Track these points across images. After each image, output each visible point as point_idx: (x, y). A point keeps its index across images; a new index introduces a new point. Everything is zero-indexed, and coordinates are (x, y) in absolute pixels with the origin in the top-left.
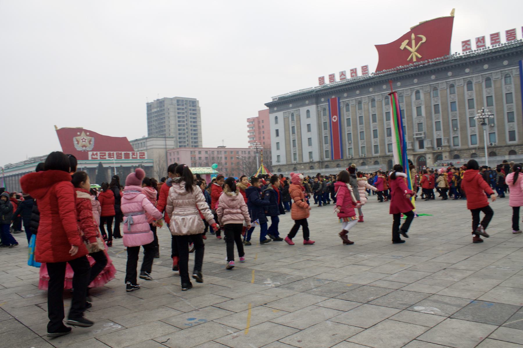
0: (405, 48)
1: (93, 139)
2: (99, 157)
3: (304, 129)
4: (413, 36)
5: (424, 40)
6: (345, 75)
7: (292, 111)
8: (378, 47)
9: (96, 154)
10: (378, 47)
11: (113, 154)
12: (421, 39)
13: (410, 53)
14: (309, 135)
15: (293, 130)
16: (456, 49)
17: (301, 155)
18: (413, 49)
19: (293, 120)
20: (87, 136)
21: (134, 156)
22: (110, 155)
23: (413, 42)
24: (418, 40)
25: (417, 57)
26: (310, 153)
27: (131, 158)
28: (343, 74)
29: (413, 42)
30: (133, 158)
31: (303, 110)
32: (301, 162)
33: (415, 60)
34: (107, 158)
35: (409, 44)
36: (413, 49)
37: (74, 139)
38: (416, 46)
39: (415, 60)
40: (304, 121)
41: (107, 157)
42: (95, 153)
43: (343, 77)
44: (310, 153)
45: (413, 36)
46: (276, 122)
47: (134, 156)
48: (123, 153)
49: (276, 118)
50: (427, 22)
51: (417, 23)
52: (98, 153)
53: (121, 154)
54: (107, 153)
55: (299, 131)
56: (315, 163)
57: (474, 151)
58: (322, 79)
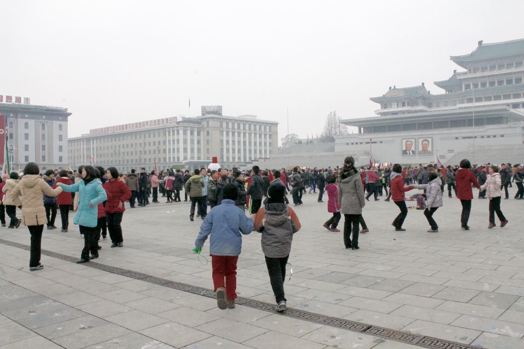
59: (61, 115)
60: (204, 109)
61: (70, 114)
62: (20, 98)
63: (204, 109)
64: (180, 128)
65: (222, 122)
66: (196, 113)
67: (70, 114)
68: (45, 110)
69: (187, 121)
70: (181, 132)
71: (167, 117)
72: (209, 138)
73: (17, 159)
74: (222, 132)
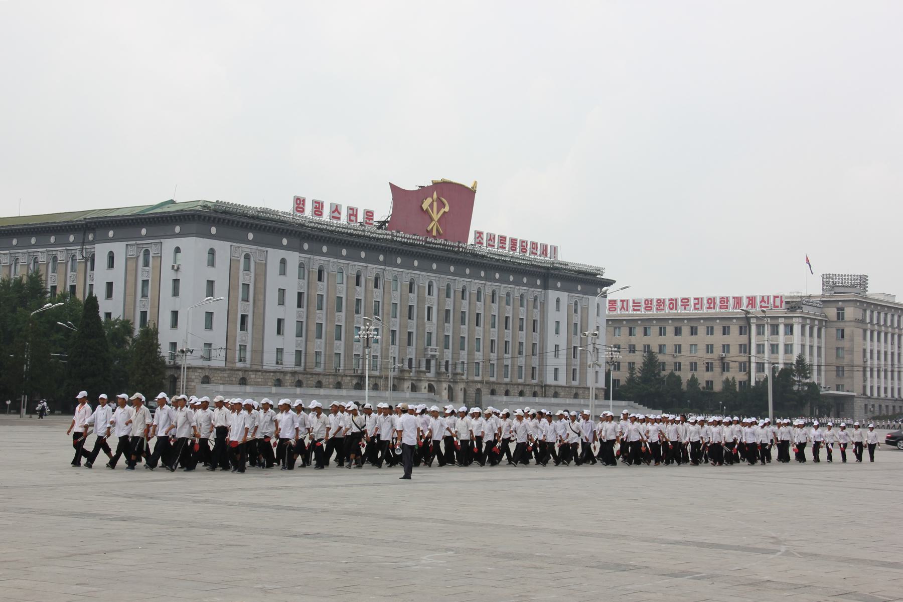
0: (427, 210)
3: (272, 296)
4: (435, 196)
5: (447, 209)
6: (340, 213)
7: (246, 248)
8: (394, 188)
10: (394, 188)
12: (444, 206)
13: (432, 219)
14: (280, 312)
15: (249, 293)
16: (471, 240)
17: (259, 351)
18: (436, 216)
19: (247, 269)
23: (435, 204)
24: (441, 205)
25: (437, 230)
26: (280, 351)
28: (336, 210)
29: (435, 204)
31: (274, 255)
32: (259, 368)
33: (434, 233)
35: (431, 205)
36: (436, 216)
38: (438, 213)
39: (434, 233)
40: (274, 281)
43: (336, 214)
44: (280, 351)
45: (435, 196)
46: (283, 272)
49: (212, 252)
50: (451, 183)
51: (438, 179)
55: (261, 297)
56: (285, 373)
57: (479, 386)
58: (299, 203)
59: (590, 282)
60: (826, 278)
61: (610, 283)
62: (546, 246)
63: (826, 278)
64: (794, 320)
65: (865, 311)
66: (815, 289)
67: (610, 283)
68: (580, 272)
69: (794, 305)
70: (797, 329)
71: (765, 293)
72: (846, 344)
73: (541, 375)
74: (865, 331)
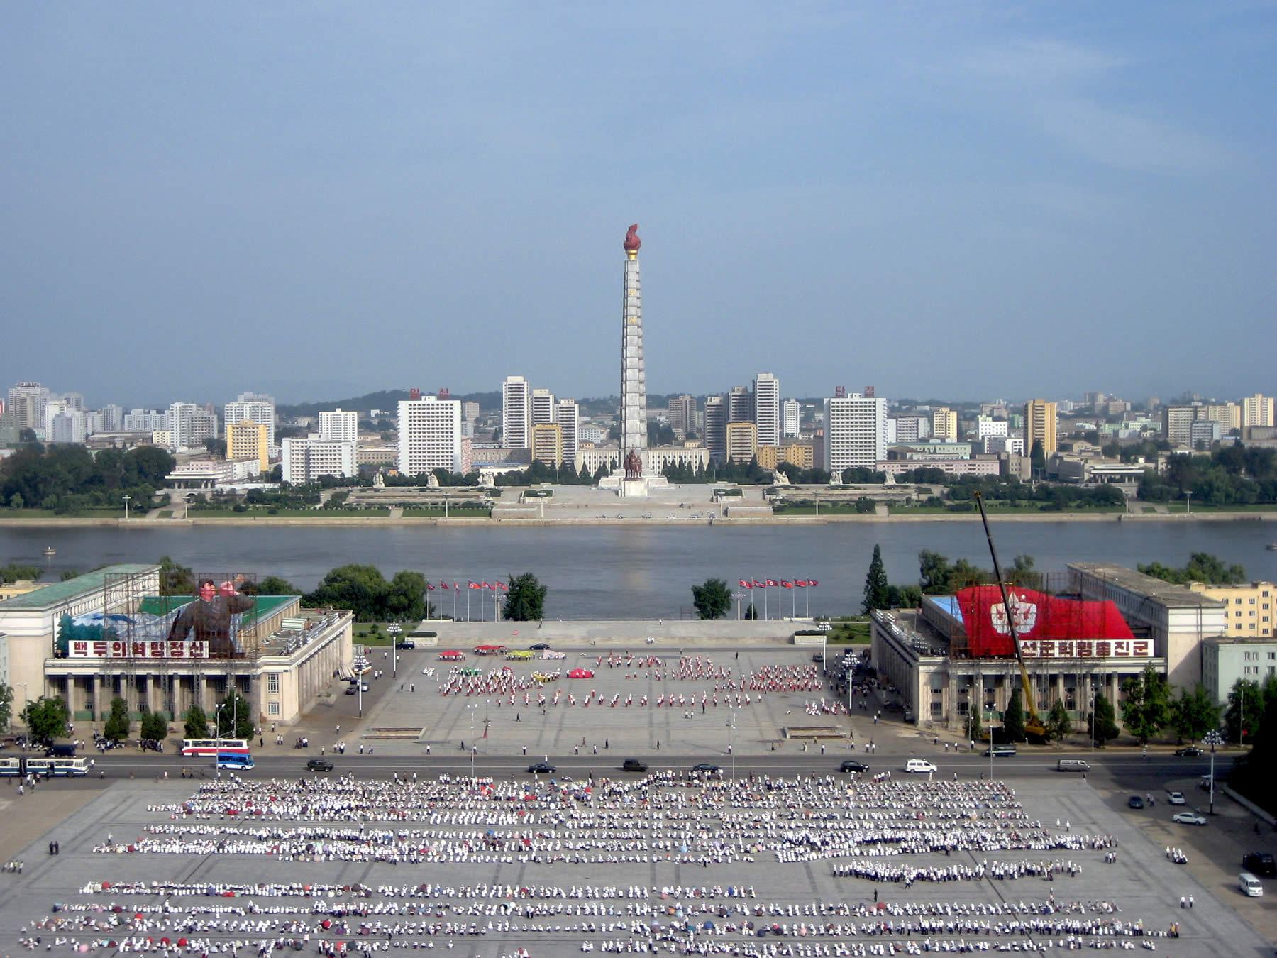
1: (1034, 608)
2: (1038, 652)
9: (1034, 646)
11: (1071, 644)
20: (1021, 601)
21: (1119, 650)
22: (1063, 648)
27: (1112, 654)
30: (1117, 653)
34: (1057, 655)
37: (994, 609)
41: (1056, 652)
42: (1029, 643)
47: (1119, 650)
48: (1094, 642)
52: (1038, 643)
53: (1090, 645)
54: (1057, 643)
